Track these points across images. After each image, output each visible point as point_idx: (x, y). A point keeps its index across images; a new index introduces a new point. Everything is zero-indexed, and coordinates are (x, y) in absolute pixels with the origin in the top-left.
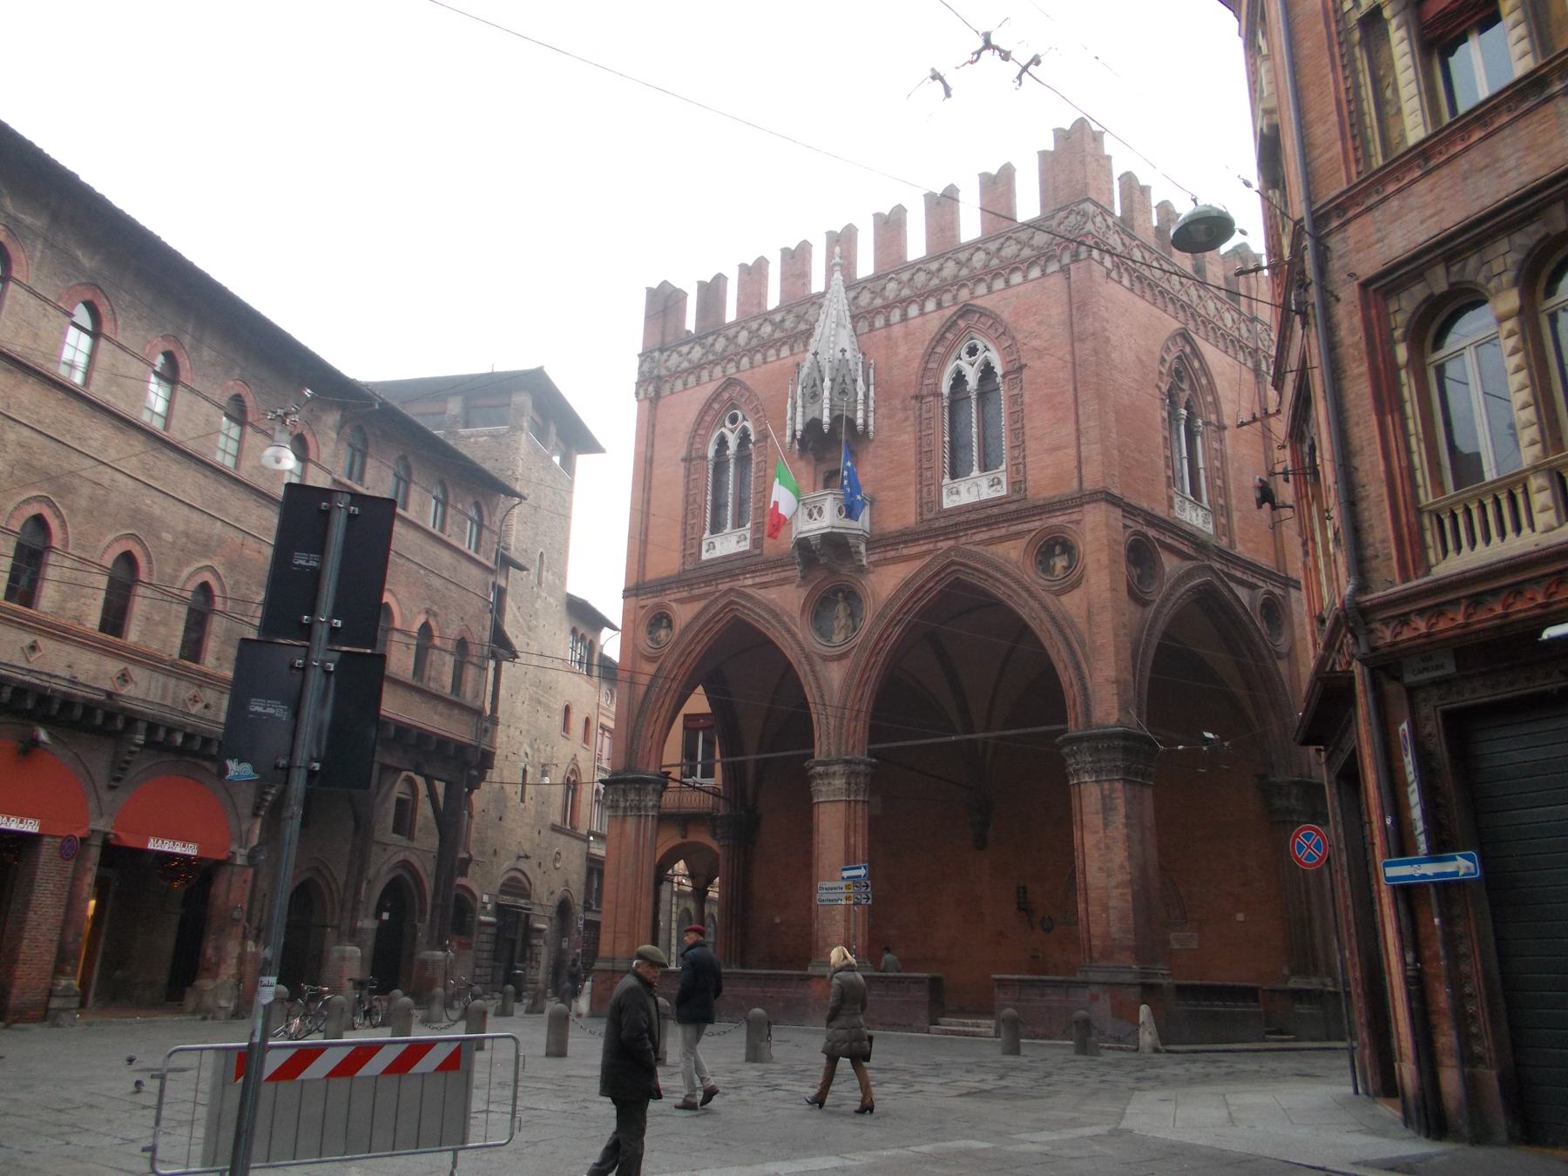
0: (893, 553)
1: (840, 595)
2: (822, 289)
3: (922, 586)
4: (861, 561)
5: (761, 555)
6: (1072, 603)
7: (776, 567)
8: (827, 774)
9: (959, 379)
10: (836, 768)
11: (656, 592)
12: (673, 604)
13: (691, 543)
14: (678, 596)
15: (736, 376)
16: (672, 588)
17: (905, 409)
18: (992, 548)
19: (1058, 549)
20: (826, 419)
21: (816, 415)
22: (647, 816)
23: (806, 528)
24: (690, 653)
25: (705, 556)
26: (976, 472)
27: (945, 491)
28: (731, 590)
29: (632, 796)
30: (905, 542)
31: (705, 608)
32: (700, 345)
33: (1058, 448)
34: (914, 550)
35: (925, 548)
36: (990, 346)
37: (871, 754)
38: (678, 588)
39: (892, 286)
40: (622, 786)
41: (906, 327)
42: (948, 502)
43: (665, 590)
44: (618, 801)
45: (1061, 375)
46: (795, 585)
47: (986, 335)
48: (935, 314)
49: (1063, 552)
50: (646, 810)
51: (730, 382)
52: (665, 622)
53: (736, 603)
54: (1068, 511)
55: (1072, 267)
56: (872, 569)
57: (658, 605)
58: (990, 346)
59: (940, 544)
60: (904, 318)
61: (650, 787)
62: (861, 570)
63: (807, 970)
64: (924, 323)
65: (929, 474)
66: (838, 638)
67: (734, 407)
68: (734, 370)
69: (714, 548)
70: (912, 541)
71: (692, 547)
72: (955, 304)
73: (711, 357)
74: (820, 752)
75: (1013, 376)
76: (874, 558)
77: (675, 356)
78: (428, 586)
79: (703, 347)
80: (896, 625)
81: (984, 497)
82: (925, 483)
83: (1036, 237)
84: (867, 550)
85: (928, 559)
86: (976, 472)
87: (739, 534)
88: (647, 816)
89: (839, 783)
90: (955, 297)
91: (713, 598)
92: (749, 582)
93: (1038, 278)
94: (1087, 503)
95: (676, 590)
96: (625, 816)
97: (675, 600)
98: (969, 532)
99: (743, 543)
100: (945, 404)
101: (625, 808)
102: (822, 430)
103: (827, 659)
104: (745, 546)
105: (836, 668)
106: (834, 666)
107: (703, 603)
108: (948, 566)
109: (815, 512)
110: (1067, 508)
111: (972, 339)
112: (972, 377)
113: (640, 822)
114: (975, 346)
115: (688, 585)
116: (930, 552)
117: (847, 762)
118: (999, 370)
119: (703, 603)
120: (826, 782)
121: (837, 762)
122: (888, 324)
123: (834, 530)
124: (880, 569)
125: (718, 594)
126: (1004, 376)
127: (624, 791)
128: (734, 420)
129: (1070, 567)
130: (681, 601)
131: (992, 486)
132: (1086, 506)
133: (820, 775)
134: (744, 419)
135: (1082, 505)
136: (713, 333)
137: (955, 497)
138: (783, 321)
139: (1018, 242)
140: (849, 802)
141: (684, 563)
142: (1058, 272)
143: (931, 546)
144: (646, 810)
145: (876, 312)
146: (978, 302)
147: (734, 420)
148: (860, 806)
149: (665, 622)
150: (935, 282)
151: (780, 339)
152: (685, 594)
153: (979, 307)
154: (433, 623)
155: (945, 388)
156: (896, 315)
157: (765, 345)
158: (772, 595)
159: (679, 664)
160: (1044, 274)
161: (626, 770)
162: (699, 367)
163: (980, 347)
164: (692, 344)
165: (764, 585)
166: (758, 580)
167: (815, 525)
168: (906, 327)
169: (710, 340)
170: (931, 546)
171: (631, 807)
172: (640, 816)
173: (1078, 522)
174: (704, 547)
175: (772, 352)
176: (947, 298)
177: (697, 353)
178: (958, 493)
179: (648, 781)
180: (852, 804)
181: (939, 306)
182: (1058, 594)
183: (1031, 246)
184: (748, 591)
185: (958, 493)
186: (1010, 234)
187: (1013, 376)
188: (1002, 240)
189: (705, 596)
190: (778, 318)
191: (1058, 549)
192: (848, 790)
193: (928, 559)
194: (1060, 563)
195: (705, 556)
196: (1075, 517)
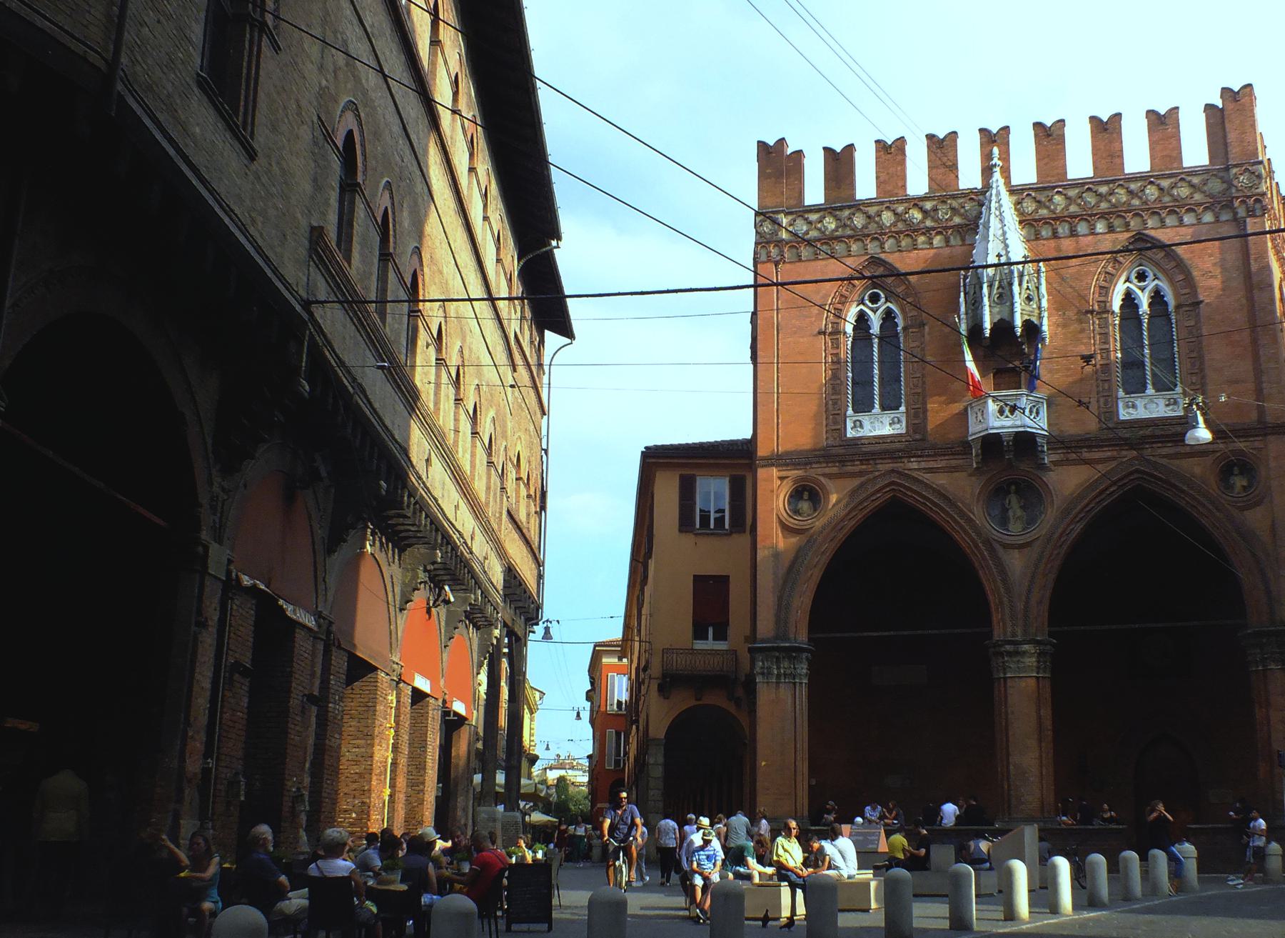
0: (1074, 456)
1: (1013, 487)
2: (978, 184)
3: (1107, 489)
4: (1044, 459)
5: (923, 440)
6: (1255, 518)
7: (944, 455)
8: (1017, 653)
9: (1129, 299)
10: (1026, 647)
11: (799, 464)
12: (822, 479)
13: (835, 419)
14: (827, 471)
15: (883, 256)
17: (1080, 321)
18: (1177, 462)
19: (1236, 470)
20: (1018, 322)
21: (1006, 316)
22: (801, 683)
23: (997, 424)
25: (850, 433)
26: (1150, 390)
27: (1121, 404)
28: (893, 471)
30: (1090, 447)
31: (862, 485)
32: (835, 216)
33: (1237, 382)
34: (1097, 455)
35: (1109, 454)
36: (1159, 275)
37: (1051, 635)
38: (827, 463)
39: (1057, 198)
40: (777, 654)
41: (1077, 243)
42: (1124, 414)
43: (811, 463)
44: (769, 668)
45: (1238, 317)
46: (964, 474)
47: (1157, 264)
48: (1107, 236)
49: (1241, 473)
50: (801, 679)
51: (875, 261)
52: (806, 495)
53: (900, 485)
54: (1252, 439)
55: (1248, 220)
56: (1053, 468)
57: (803, 479)
58: (1159, 275)
59: (1124, 453)
60: (1073, 233)
61: (804, 655)
62: (1042, 467)
63: (993, 825)
64: (1096, 243)
65: (1106, 386)
66: (1015, 527)
67: (875, 286)
68: (878, 250)
69: (861, 426)
70: (1096, 447)
71: (835, 423)
72: (1128, 231)
73: (849, 232)
74: (998, 634)
75: (1187, 309)
76: (1055, 457)
77: (799, 222)
79: (838, 219)
80: (1078, 522)
81: (1162, 414)
82: (1101, 394)
83: (1210, 185)
84: (1048, 449)
85: (1114, 464)
86: (1150, 390)
87: (892, 416)
88: (801, 683)
89: (1031, 661)
90: (1127, 224)
91: (871, 476)
92: (915, 466)
93: (1211, 223)
94: (1270, 434)
95: (825, 465)
96: (778, 683)
97: (824, 475)
98: (1154, 445)
99: (898, 426)
100: (1117, 322)
101: (779, 676)
102: (1015, 333)
103: (1006, 546)
104: (901, 429)
105: (1018, 556)
106: (1016, 553)
107: (856, 482)
108: (1131, 473)
109: (1007, 409)
110: (1247, 436)
111: (1140, 265)
112: (1144, 301)
113: (795, 687)
114: (1144, 272)
115: (839, 462)
116: (1114, 458)
117: (1038, 643)
118: (1170, 299)
119: (856, 482)
120: (1015, 659)
121: (1029, 642)
122: (1055, 235)
123: (1029, 430)
124: (1060, 468)
125: (877, 473)
126: (1178, 307)
127: (778, 658)
128: (875, 298)
129: (1250, 486)
130: (830, 476)
131: (1167, 405)
132: (1269, 437)
133: (1010, 654)
134: (887, 300)
135: (1266, 435)
136: (849, 207)
137: (1131, 410)
138: (935, 210)
139: (1192, 186)
141: (827, 438)
142: (1232, 221)
143: (1115, 453)
145: (1043, 220)
146: (1152, 233)
147: (875, 298)
149: (806, 495)
150: (1104, 205)
151: (934, 229)
152: (835, 470)
153: (1152, 238)
155: (1116, 304)
156: (1063, 229)
157: (913, 230)
158: (941, 480)
160: (1217, 220)
161: (777, 638)
162: (829, 239)
163: (1151, 276)
164: (822, 213)
165: (931, 470)
166: (923, 465)
167: (1008, 422)
168: (1077, 243)
169: (847, 213)
170: (1115, 453)
171: (785, 675)
172: (795, 683)
173: (1259, 449)
174: (849, 424)
175: (922, 239)
176: (1117, 223)
177: (830, 223)
178: (1134, 406)
179: (800, 650)
181: (1111, 229)
182: (1242, 509)
183: (1204, 192)
184: (914, 474)
185: (1134, 406)
186: (1183, 176)
187: (1187, 309)
188: (1173, 180)
189: (861, 474)
190: (928, 205)
191: (1236, 470)
192: (1038, 668)
193: (1114, 464)
194: (1239, 482)
195: (850, 433)
196: (1256, 444)
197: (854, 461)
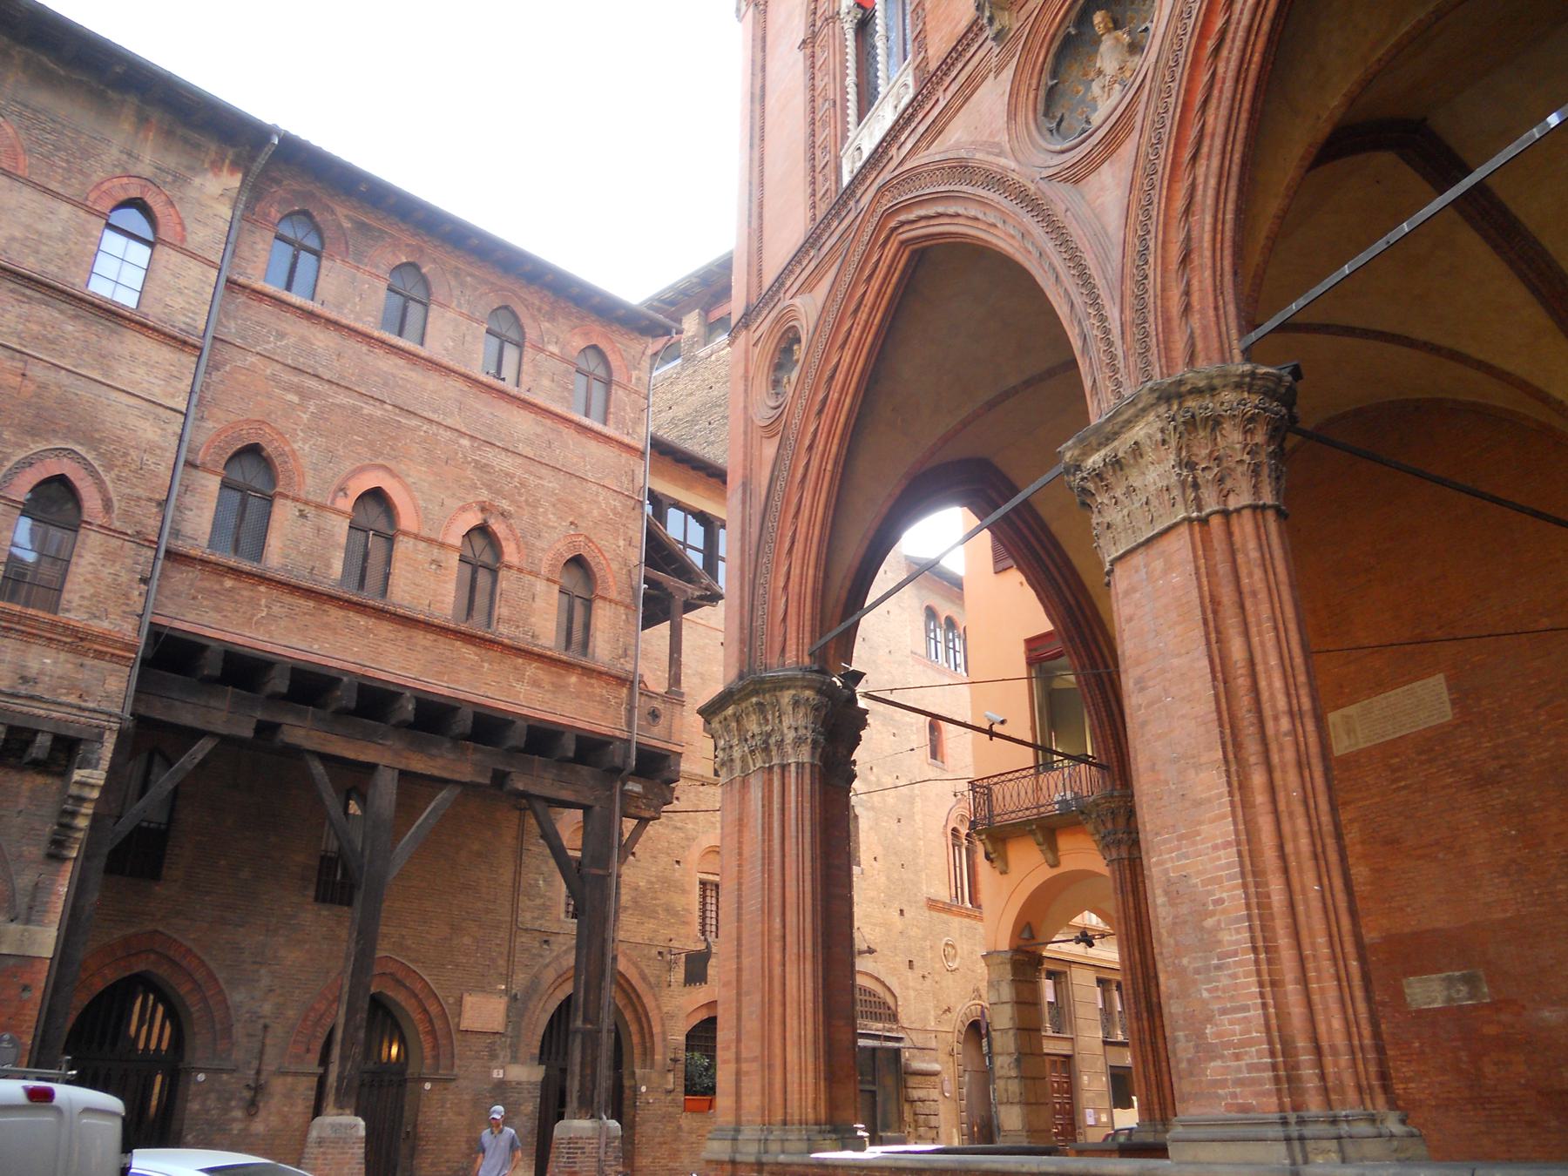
10: (1139, 432)
11: (772, 298)
16: (792, 272)
24: (832, 377)
29: (753, 725)
57: (778, 320)
61: (786, 697)
78: (483, 467)
88: (784, 768)
89: (1157, 473)
113: (771, 780)
140: (1204, 521)
144: (783, 755)
148: (1245, 528)
154: (497, 526)
159: (816, 408)
172: (771, 768)
179: (779, 685)
180: (1216, 521)
197: (829, 225)
